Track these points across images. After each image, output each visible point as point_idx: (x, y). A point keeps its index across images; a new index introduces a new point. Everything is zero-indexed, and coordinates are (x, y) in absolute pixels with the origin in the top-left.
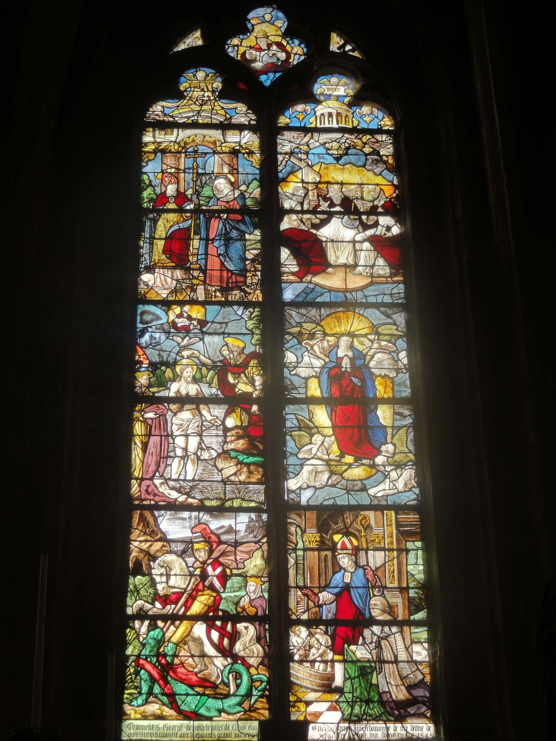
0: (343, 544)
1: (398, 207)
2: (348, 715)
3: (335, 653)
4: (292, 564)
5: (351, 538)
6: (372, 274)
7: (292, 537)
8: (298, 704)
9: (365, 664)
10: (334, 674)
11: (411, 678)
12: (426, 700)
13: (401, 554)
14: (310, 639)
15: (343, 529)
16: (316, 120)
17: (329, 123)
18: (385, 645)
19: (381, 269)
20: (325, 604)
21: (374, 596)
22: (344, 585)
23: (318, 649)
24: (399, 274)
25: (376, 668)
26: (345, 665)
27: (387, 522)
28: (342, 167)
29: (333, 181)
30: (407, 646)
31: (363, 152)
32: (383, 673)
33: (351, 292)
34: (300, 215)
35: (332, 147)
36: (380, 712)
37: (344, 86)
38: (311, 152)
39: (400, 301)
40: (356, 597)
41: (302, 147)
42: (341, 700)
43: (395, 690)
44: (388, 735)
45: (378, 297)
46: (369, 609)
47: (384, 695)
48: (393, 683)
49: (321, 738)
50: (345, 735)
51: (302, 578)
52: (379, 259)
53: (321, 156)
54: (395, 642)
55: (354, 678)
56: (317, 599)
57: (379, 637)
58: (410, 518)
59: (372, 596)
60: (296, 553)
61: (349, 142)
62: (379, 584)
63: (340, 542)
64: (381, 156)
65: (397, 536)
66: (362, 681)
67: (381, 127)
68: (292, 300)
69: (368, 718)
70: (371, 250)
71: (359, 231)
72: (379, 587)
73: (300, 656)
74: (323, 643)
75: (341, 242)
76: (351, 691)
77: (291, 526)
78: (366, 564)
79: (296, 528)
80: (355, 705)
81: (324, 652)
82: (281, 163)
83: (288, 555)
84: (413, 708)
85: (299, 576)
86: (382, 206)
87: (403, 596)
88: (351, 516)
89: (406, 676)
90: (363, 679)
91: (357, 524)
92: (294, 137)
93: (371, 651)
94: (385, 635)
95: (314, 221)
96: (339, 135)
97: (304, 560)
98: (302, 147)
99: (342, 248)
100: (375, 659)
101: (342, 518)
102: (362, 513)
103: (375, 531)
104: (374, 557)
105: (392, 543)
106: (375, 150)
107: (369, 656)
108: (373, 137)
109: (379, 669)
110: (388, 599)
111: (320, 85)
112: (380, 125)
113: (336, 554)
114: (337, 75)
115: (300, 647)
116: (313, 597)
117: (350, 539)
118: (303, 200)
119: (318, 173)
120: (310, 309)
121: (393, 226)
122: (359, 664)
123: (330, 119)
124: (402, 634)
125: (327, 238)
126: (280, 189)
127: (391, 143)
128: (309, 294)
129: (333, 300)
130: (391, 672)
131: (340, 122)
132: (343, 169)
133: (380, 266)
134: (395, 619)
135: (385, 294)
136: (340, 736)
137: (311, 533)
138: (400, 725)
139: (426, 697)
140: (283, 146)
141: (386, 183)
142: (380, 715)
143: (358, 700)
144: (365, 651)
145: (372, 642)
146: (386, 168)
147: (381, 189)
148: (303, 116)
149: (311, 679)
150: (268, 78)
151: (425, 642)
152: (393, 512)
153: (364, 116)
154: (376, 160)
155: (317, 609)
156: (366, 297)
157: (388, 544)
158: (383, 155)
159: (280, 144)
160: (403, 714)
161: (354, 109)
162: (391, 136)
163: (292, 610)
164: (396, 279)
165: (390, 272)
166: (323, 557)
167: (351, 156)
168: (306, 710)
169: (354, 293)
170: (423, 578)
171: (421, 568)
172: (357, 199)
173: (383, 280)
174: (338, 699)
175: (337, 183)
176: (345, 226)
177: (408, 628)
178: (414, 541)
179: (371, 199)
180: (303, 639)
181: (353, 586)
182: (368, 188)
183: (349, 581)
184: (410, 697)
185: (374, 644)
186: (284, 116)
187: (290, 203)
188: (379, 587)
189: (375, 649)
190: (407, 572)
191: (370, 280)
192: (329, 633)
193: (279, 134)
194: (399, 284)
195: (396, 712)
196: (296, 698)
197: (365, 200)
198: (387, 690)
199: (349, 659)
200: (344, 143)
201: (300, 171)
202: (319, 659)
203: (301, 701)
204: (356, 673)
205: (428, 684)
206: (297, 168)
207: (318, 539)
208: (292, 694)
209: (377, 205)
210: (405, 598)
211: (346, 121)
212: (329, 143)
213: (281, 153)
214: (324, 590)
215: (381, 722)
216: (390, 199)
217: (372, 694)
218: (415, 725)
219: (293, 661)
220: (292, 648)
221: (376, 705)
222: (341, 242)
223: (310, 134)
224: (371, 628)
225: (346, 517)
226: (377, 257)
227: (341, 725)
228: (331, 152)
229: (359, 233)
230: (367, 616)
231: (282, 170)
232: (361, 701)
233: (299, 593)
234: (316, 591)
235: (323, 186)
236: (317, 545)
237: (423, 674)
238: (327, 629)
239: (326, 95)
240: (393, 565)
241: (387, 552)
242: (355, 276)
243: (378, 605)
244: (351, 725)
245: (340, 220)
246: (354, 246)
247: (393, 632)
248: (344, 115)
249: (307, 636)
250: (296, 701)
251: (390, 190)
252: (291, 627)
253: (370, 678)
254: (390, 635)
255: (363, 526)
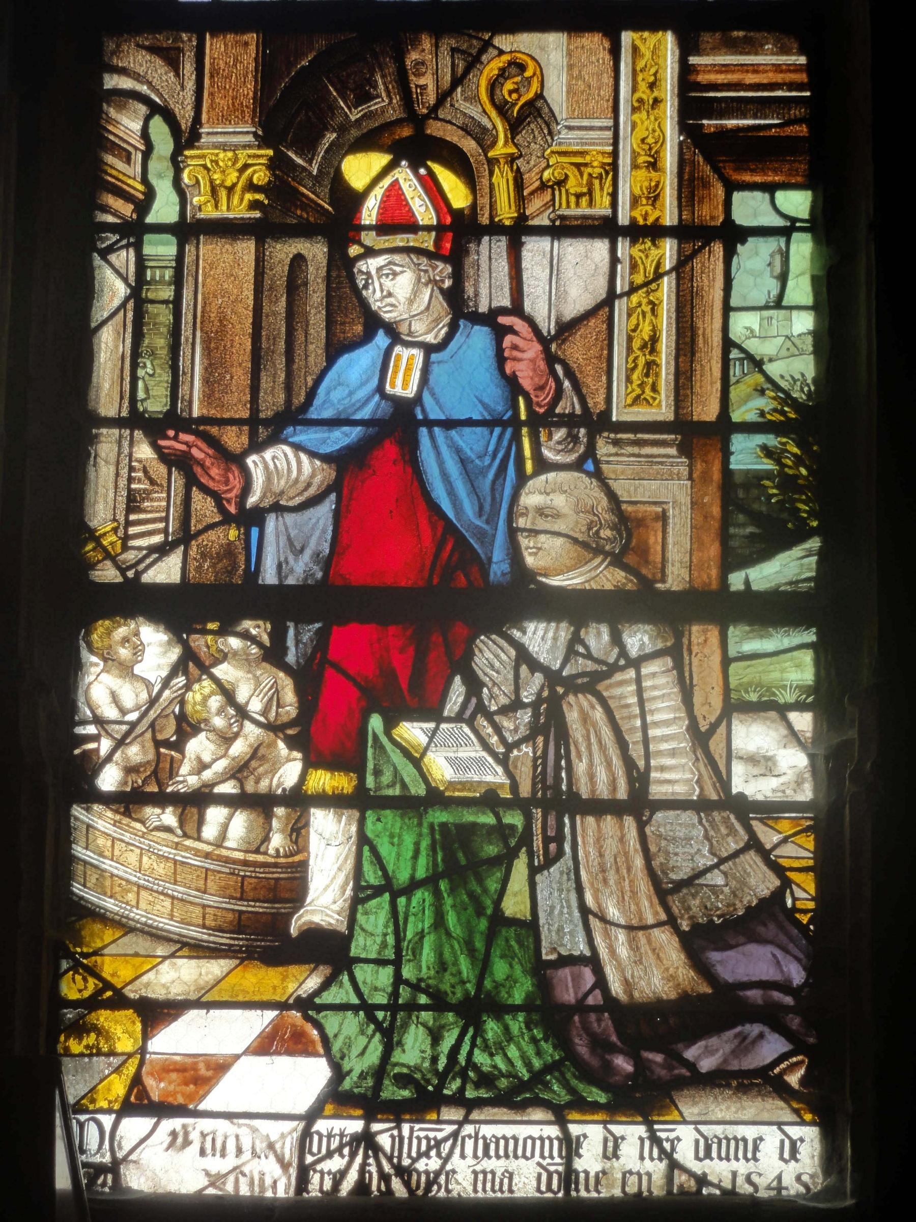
0: (395, 194)
2: (362, 1076)
3: (310, 763)
4: (116, 303)
5: (437, 169)
7: (120, 165)
8: (103, 1017)
9: (469, 816)
10: (303, 866)
11: (714, 888)
12: (789, 1000)
13: (695, 253)
14: (188, 687)
15: (399, 122)
18: (585, 718)
20: (277, 508)
21: (543, 466)
22: (386, 409)
23: (227, 739)
25: (526, 839)
26: (362, 822)
27: (634, 89)
30: (704, 727)
32: (566, 861)
36: (537, 1064)
40: (445, 477)
42: (331, 996)
43: (623, 951)
44: (569, 1177)
46: (512, 532)
47: (565, 973)
48: (613, 912)
49: (211, 1191)
50: (337, 1184)
51: (167, 377)
54: (641, 702)
55: (414, 885)
56: (236, 482)
57: (552, 677)
58: (755, 69)
59: (529, 466)
60: (138, 247)
62: (569, 404)
63: (378, 193)
65: (682, 163)
66: (448, 901)
69: (470, 1094)
72: (570, 421)
73: (130, 770)
74: (255, 706)
76: (390, 954)
77: (121, 107)
78: (506, 302)
79: (147, 120)
80: (405, 1026)
81: (255, 753)
83: (97, 260)
84: (714, 1041)
85: (147, 368)
87: (699, 466)
88: (446, 61)
89: (688, 882)
90: (452, 891)
91: (474, 99)
93: (509, 747)
94: (590, 666)
97: (178, 281)
100: (525, 790)
101: (391, 68)
102: (503, 41)
103: (564, 134)
104: (554, 268)
105: (654, 196)
107: (495, 776)
109: (547, 840)
110: (621, 488)
113: (354, 250)
115: (133, 725)
116: (215, 472)
117: (431, 174)
122: (439, 816)
124: (679, 666)
130: (609, 860)
134: (646, 584)
136: (315, 1179)
137: (224, 147)
138: (641, 1130)
139: (784, 987)
142: (538, 1078)
143: (423, 999)
144: (475, 752)
145: (516, 705)
149: (179, 890)
151: (799, 706)
152: (669, 41)
155: (233, 534)
157: (635, 201)
160: (663, 1073)
163: (97, 540)
166: (279, 270)
168: (143, 1051)
170: (810, 373)
171: (804, 323)
174: (318, 992)
177: (713, 634)
178: (770, 189)
180: (148, 684)
181: (435, 414)
183: (410, 392)
184: (705, 989)
185: (525, 716)
188: (570, 421)
189: (529, 739)
190: (728, 344)
192: (291, 658)
195: (623, 1064)
196: (92, 983)
198: (582, 948)
199: (390, 792)
202: (228, 788)
203: (119, 1001)
204: (422, 861)
205: (805, 919)
207: (261, 176)
208: (76, 966)
210: (706, 477)
214: (275, 439)
215: (538, 1114)
217: (500, 969)
218: (718, 1130)
219: (93, 796)
220: (91, 729)
221: (516, 1024)
224: (516, 634)
225: (420, 63)
227: (322, 1125)
230: (499, 567)
232: (439, 1004)
233: (144, 451)
234: (234, 439)
236: (254, 205)
237: (778, 869)
238: (278, 636)
240: (654, 306)
241: (623, 247)
243: (557, 515)
244: (376, 1127)
247: (634, 652)
249: (173, 673)
250: (93, 1003)
252: (88, 624)
253: (493, 885)
254: (614, 668)
255: (502, 109)
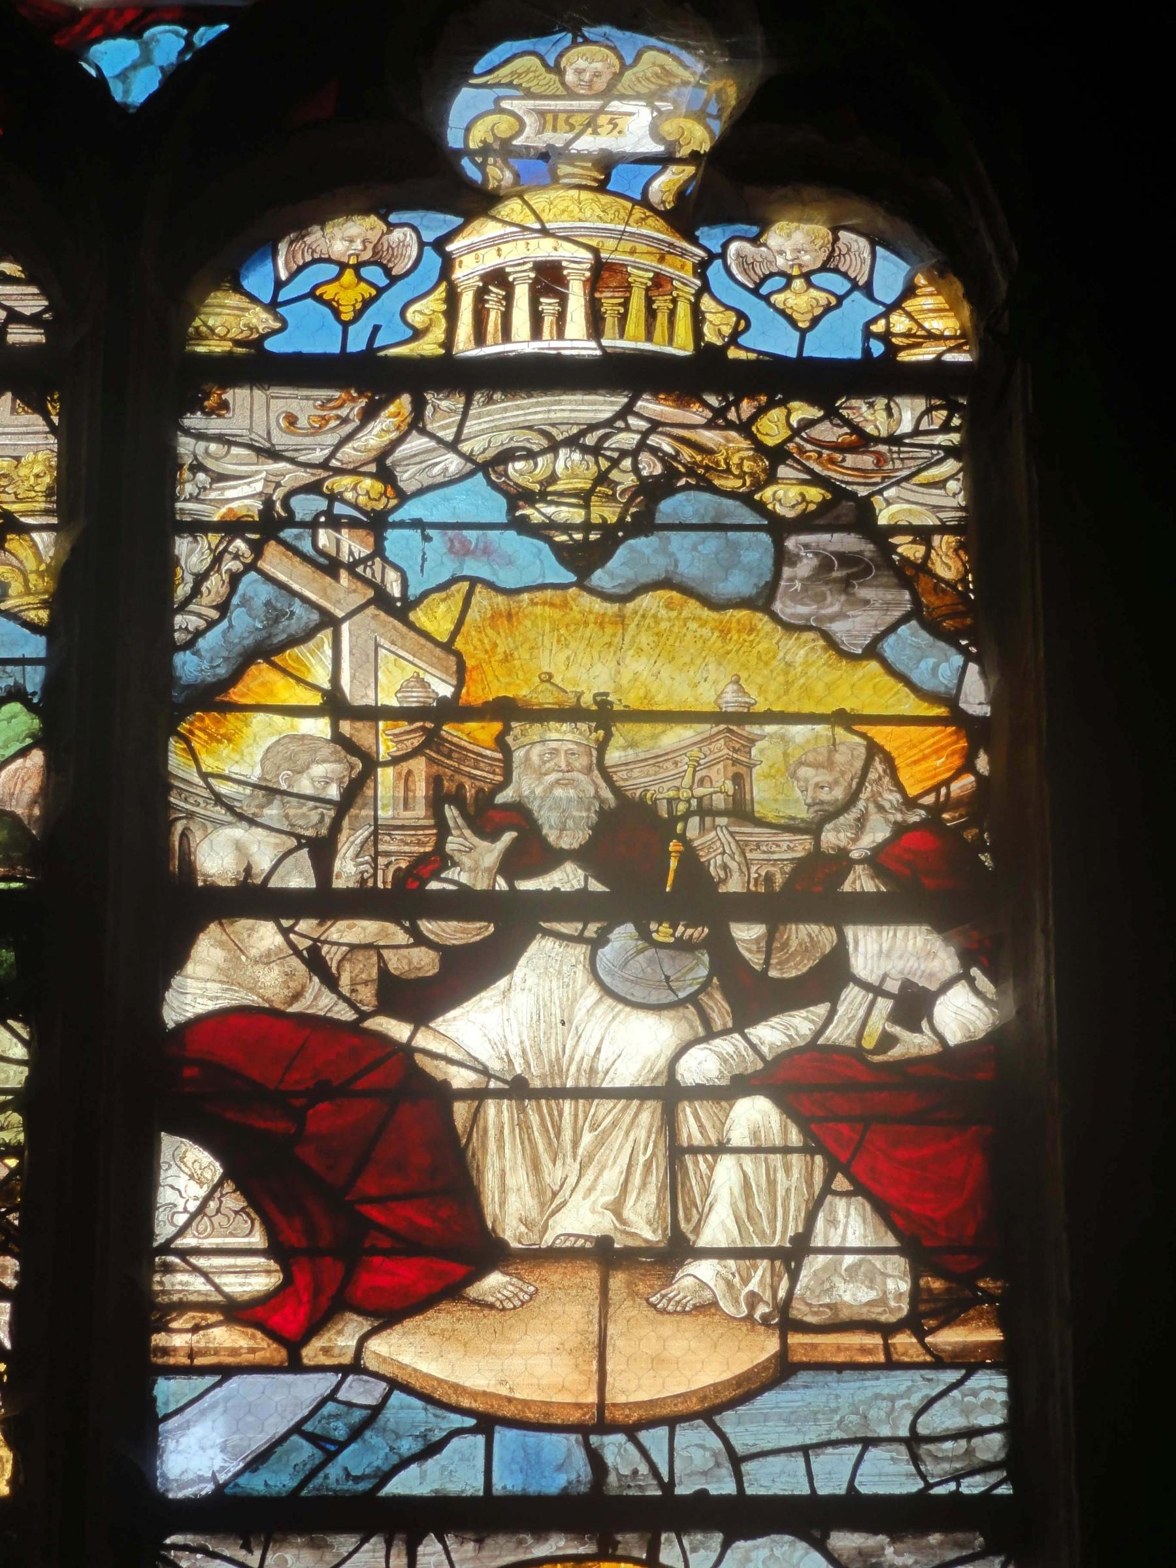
1: (986, 859)
6: (784, 1308)
16: (451, 314)
17: (536, 332)
19: (852, 1271)
24: (975, 1302)
28: (612, 608)
29: (546, 699)
31: (760, 508)
33: (631, 1431)
34: (304, 926)
35: (553, 478)
37: (649, 99)
38: (410, 511)
39: (973, 1486)
41: (342, 484)
45: (822, 1462)
52: (841, 1204)
53: (471, 535)
61: (667, 446)
64: (881, 537)
67: (892, 350)
68: (220, 1488)
70: (786, 1150)
71: (706, 1021)
75: (576, 1094)
82: (196, 591)
86: (876, 860)
92: (292, 420)
95: (396, 963)
96: (603, 406)
98: (342, 484)
99: (587, 1138)
106: (839, 494)
108: (832, 413)
111: (490, 95)
112: (886, 337)
114: (606, 29)
118: (336, 827)
119: (447, 647)
120: (344, 1543)
121: (946, 987)
123: (548, 304)
125: (485, 1072)
126: (177, 761)
127: (951, 452)
128: (342, 1446)
129: (505, 1482)
131: (610, 323)
132: (621, 620)
133: (841, 1251)
135: (868, 1442)
140: (221, 477)
141: (911, 705)
146: (916, 613)
147: (873, 749)
148: (368, 291)
150: (146, 59)
153: (779, 282)
154: (846, 559)
156: (736, 1461)
158: (896, 529)
159: (197, 467)
161: (711, 237)
162: (952, 408)
164: (949, 1338)
165: (916, 1294)
167: (676, 539)
169: (656, 1439)
172: (705, 811)
173: (863, 1350)
175: (571, 714)
176: (607, 991)
179: (803, 813)
182: (783, 738)
186: (238, 289)
187: (239, 847)
191: (772, 1345)
193: (195, 405)
194: (971, 1370)
197: (760, 823)
200: (634, 453)
201: (325, 636)
206: (303, 616)
209: (843, 853)
211: (651, 314)
212: (531, 455)
213: (198, 527)
216: (935, 810)
222: (576, 1094)
223: (405, 400)
226: (827, 1190)
228: (535, 514)
229: (710, 1035)
231: (199, 634)
235: (483, 732)
239: (524, 152)
242: (668, 1327)
245: (580, 952)
246: (670, 1123)
248: (640, 278)
251: (937, 752)
